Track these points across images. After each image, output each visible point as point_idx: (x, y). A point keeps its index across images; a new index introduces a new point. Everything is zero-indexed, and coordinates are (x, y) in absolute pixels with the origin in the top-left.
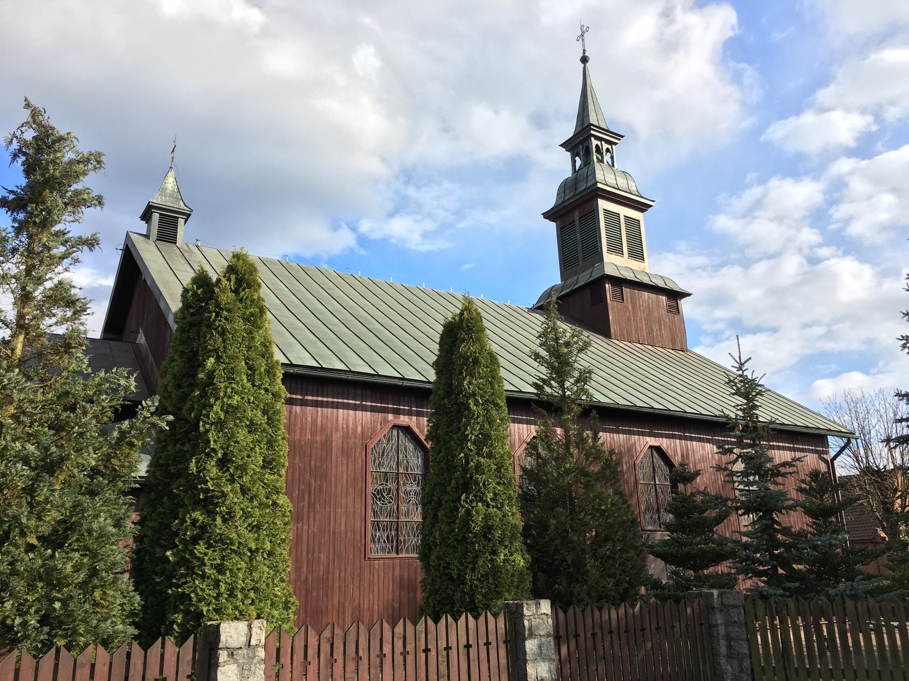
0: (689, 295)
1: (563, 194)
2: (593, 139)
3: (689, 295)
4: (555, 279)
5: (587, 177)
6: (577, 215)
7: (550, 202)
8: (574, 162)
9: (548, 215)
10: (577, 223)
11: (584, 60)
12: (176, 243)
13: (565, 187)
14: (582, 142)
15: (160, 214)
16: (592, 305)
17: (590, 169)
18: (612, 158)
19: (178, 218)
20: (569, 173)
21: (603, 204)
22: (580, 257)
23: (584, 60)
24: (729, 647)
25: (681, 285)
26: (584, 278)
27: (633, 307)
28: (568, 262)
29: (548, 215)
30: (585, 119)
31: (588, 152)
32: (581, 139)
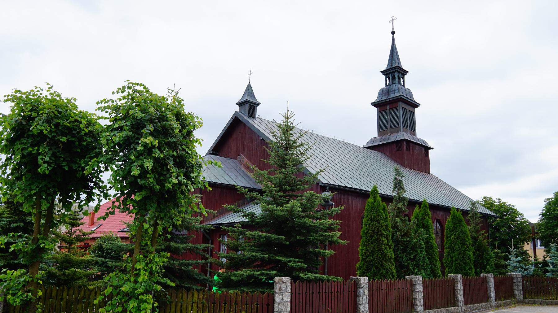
0: (433, 149)
1: (381, 96)
2: (397, 72)
3: (433, 149)
4: (374, 133)
5: (395, 90)
6: (388, 107)
7: (374, 98)
8: (386, 81)
9: (374, 104)
10: (388, 111)
11: (393, 33)
12: (254, 118)
13: (382, 92)
14: (391, 73)
15: (249, 105)
16: (396, 151)
17: (396, 87)
18: (403, 81)
19: (254, 106)
20: (383, 86)
21: (401, 105)
22: (389, 127)
23: (393, 33)
24: (518, 288)
25: (430, 145)
26: (393, 138)
27: (413, 153)
28: (382, 128)
29: (374, 104)
30: (393, 62)
31: (394, 78)
32: (391, 71)
